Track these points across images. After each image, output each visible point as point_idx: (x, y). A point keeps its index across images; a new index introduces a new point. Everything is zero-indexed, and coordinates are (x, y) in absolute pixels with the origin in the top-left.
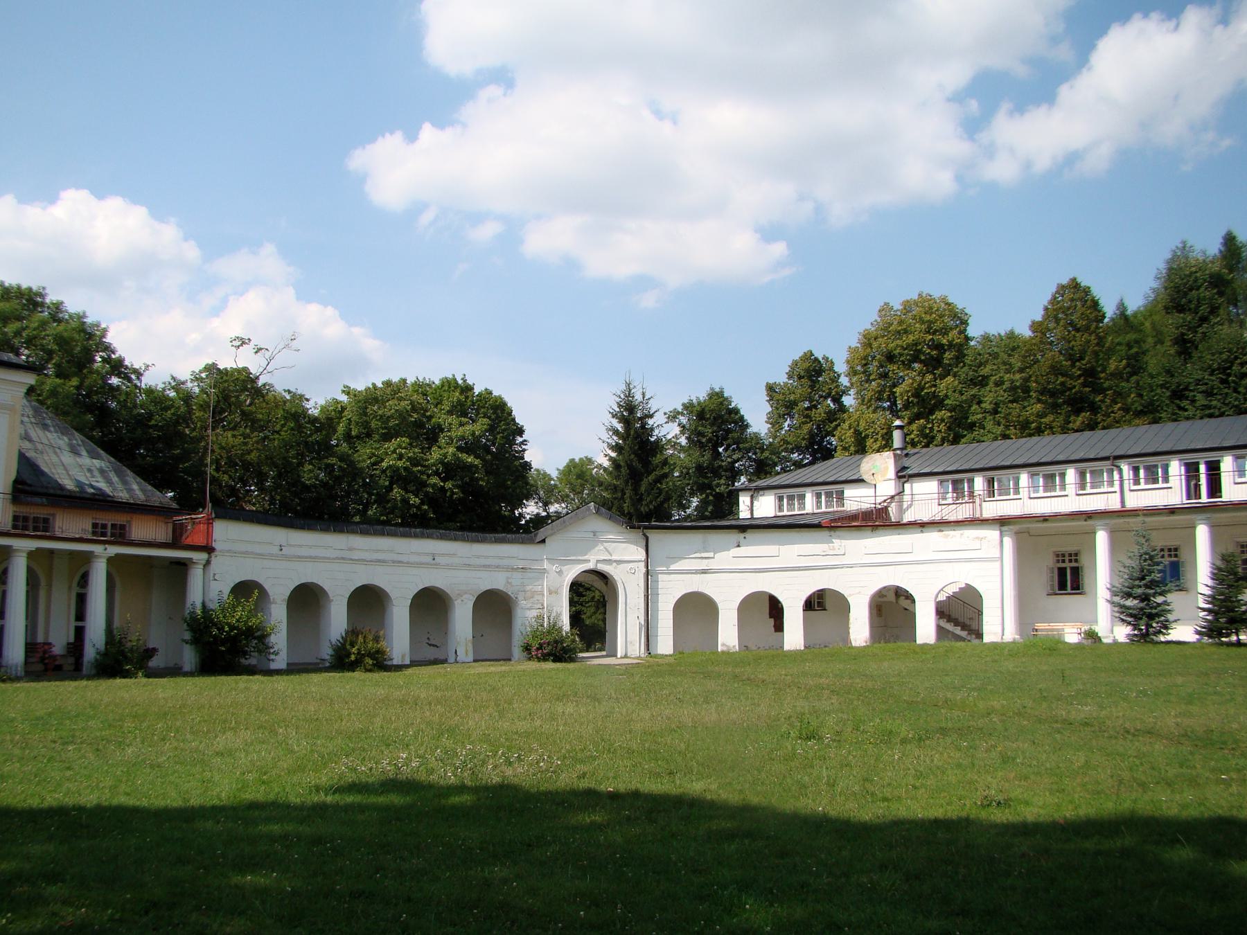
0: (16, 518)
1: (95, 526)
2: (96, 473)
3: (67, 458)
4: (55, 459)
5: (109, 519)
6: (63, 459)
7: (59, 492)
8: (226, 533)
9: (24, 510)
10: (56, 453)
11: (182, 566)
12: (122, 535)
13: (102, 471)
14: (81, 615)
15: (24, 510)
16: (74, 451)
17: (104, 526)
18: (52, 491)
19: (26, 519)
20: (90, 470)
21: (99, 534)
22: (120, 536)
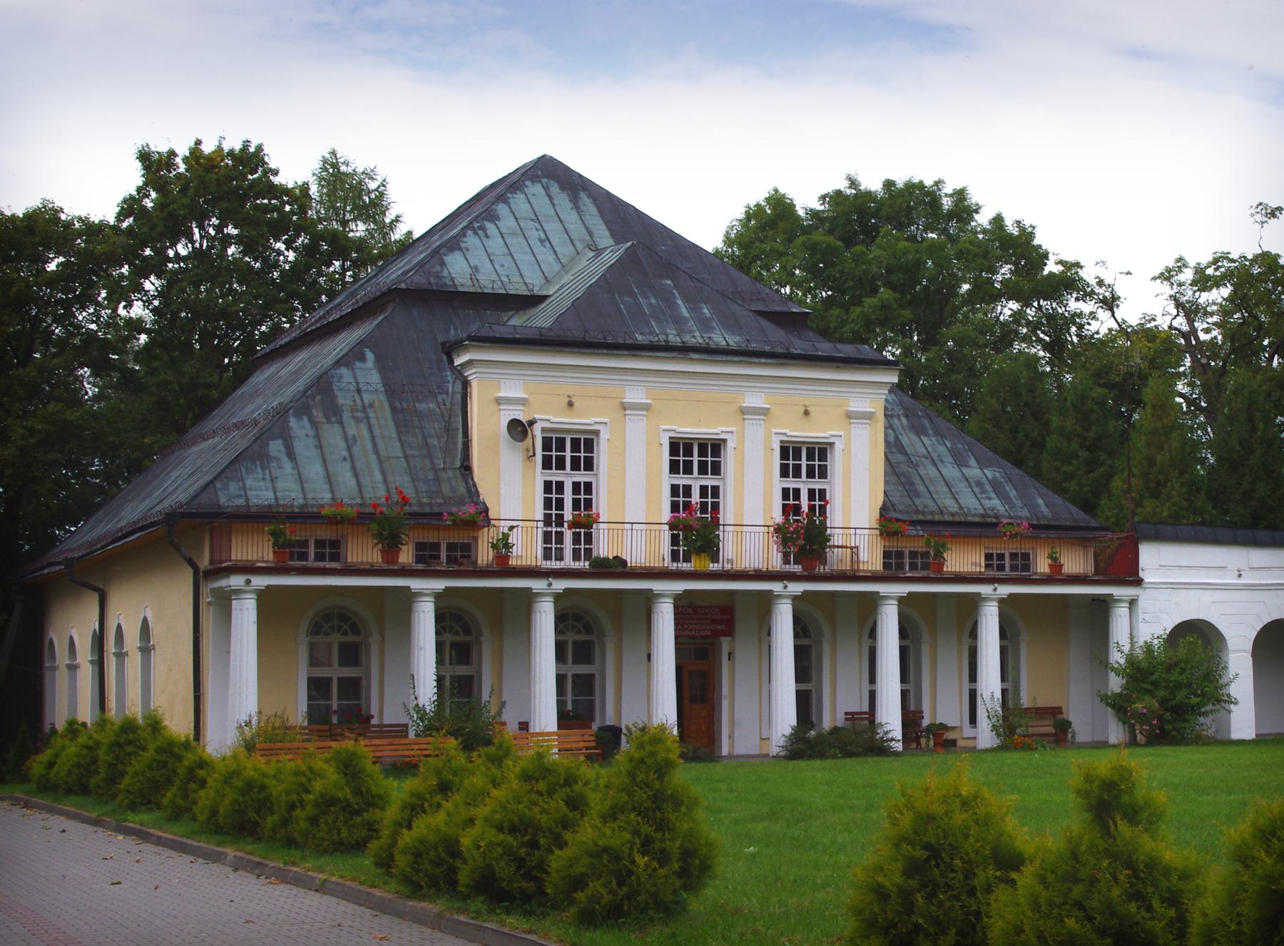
0: (887, 555)
1: (988, 557)
2: (988, 487)
3: (950, 471)
4: (932, 472)
5: (1005, 548)
6: (944, 471)
7: (938, 518)
8: (1155, 559)
9: (895, 545)
10: (935, 465)
11: (1103, 606)
12: (1026, 567)
13: (995, 484)
14: (973, 677)
15: (895, 545)
16: (960, 462)
17: (1001, 557)
18: (929, 518)
19: (900, 555)
20: (979, 484)
21: (994, 571)
22: (1021, 570)
